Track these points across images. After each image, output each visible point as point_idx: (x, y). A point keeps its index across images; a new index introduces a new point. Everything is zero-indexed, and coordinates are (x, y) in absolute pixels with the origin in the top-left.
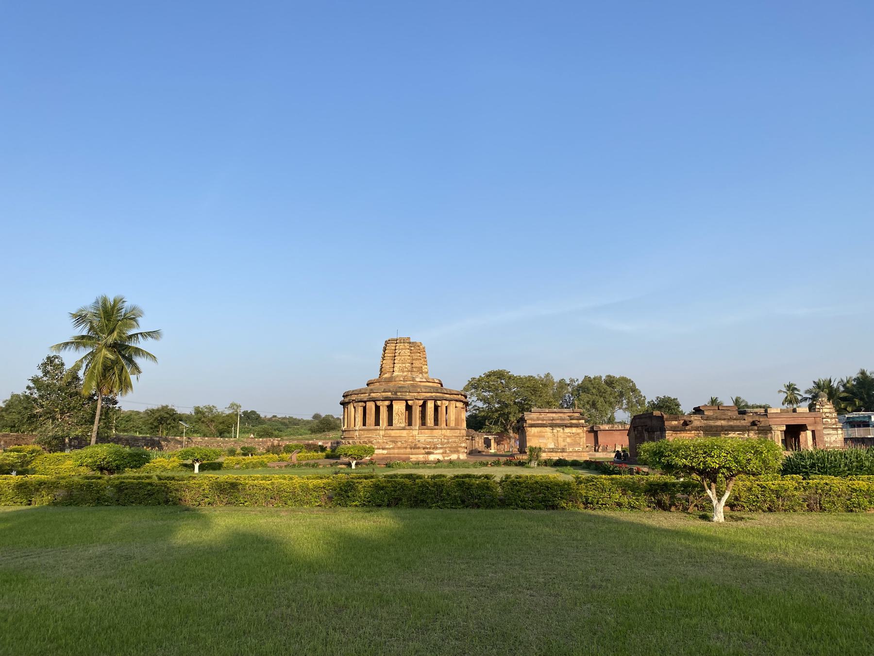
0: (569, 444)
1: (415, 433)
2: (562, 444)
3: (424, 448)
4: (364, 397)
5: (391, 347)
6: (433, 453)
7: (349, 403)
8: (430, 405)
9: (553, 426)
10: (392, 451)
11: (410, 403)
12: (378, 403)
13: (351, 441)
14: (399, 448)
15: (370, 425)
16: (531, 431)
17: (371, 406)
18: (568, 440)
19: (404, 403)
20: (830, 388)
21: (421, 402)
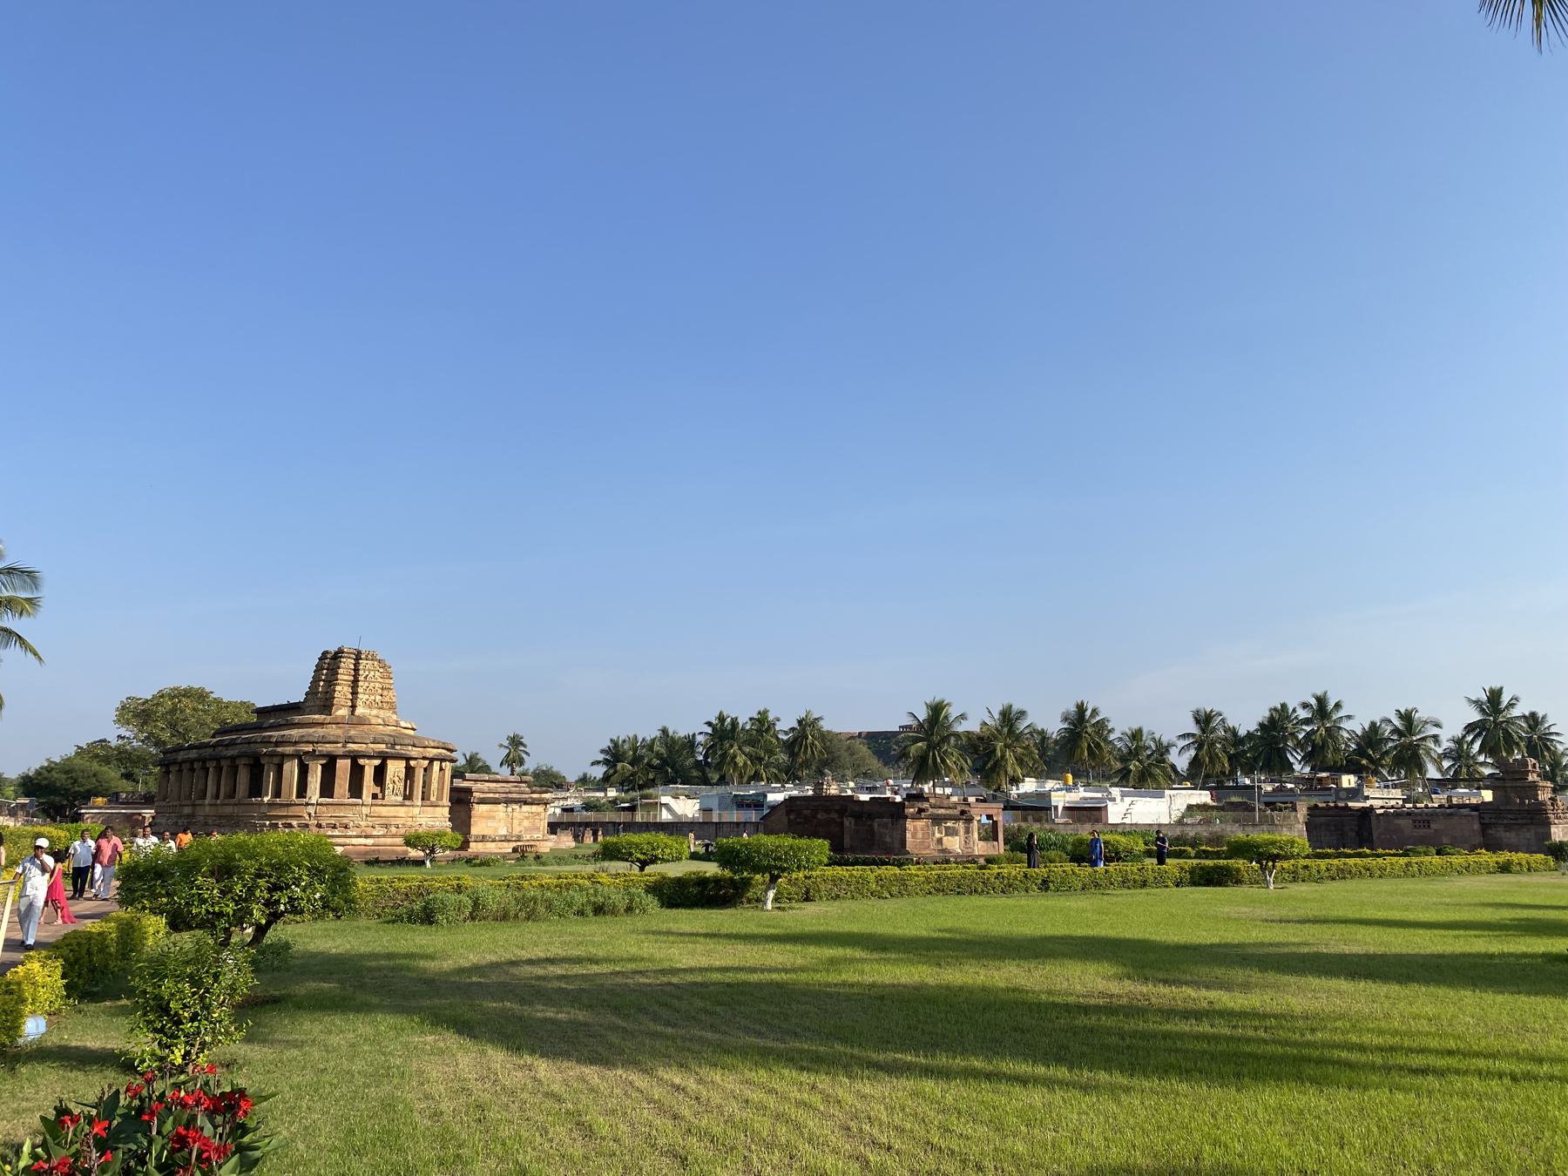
0: (526, 829)
1: (416, 811)
2: (516, 832)
4: (337, 749)
5: (347, 664)
7: (292, 756)
9: (508, 802)
10: (382, 840)
11: (412, 763)
12: (361, 761)
13: (294, 823)
16: (479, 810)
17: (343, 766)
18: (526, 823)
19: (403, 764)
20: (635, 749)
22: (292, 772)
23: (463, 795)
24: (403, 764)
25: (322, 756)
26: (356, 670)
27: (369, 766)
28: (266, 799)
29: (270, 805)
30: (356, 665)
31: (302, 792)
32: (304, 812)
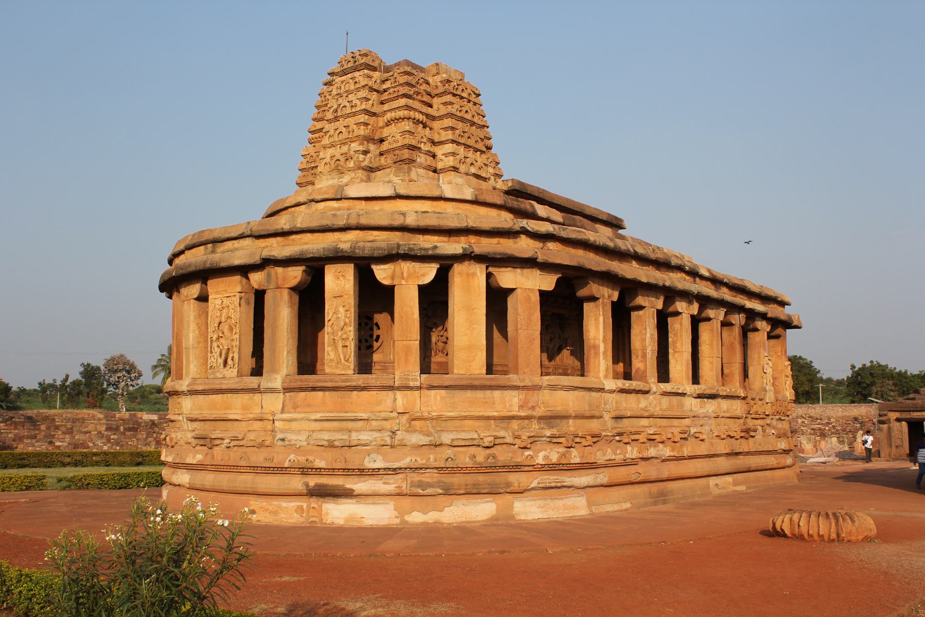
1: (273, 403)
3: (305, 471)
6: (348, 494)
8: (340, 284)
14: (218, 468)
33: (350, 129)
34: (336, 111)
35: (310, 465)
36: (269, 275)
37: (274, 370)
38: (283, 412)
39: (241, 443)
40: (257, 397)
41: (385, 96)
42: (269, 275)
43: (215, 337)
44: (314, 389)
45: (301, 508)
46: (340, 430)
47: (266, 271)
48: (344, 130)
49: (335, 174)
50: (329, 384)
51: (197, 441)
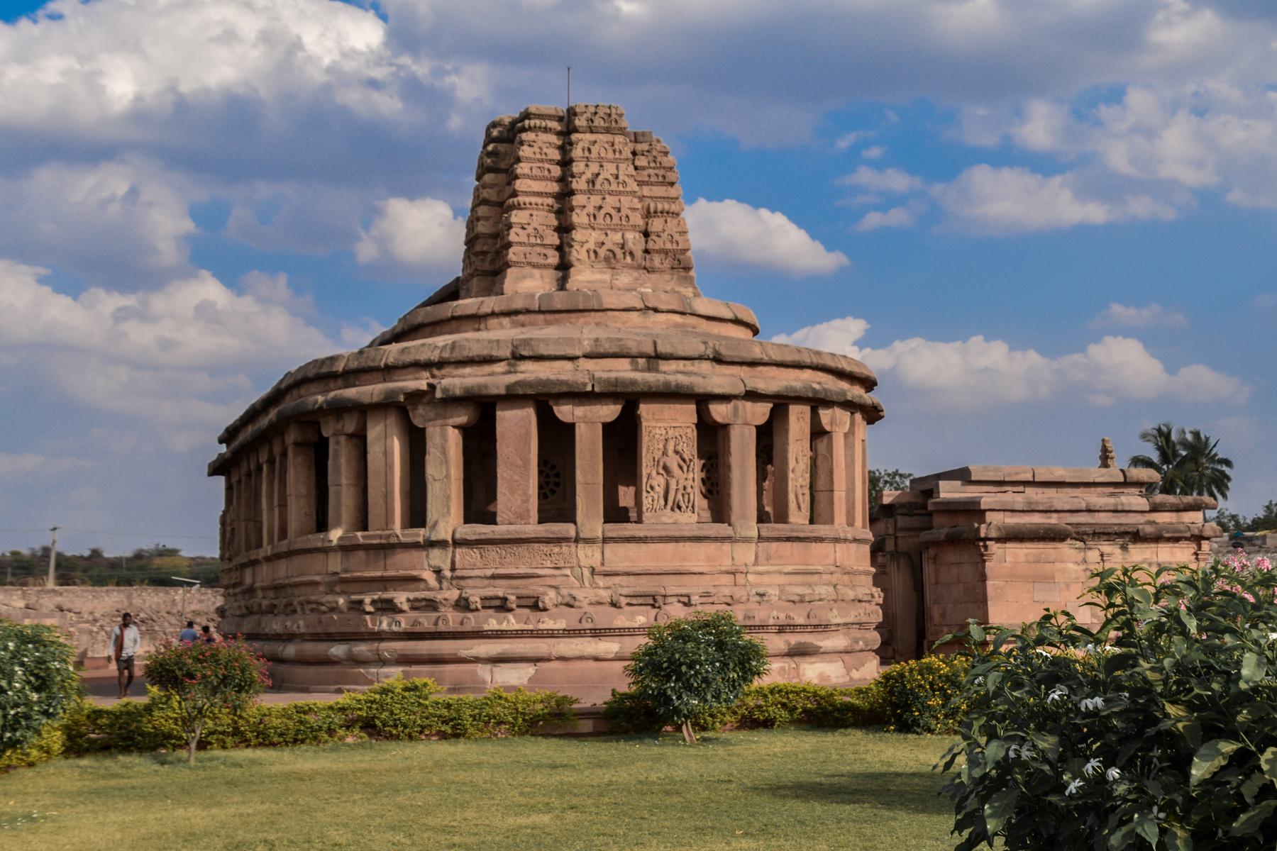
1: (745, 554)
3: (781, 629)
11: (719, 412)
12: (564, 412)
15: (522, 517)
17: (517, 430)
19: (686, 415)
21: (761, 412)
22: (387, 453)
23: (962, 524)
24: (686, 415)
25: (452, 401)
26: (566, 163)
27: (587, 423)
28: (335, 535)
29: (346, 548)
30: (565, 148)
31: (416, 514)
32: (424, 566)
33: (623, 213)
34: (592, 182)
35: (792, 622)
36: (736, 408)
37: (744, 517)
38: (756, 563)
39: (710, 600)
40: (726, 547)
41: (643, 176)
42: (736, 408)
43: (654, 473)
44: (789, 539)
45: (783, 669)
46: (803, 585)
47: (733, 403)
48: (613, 213)
49: (603, 264)
50: (801, 535)
51: (628, 600)
